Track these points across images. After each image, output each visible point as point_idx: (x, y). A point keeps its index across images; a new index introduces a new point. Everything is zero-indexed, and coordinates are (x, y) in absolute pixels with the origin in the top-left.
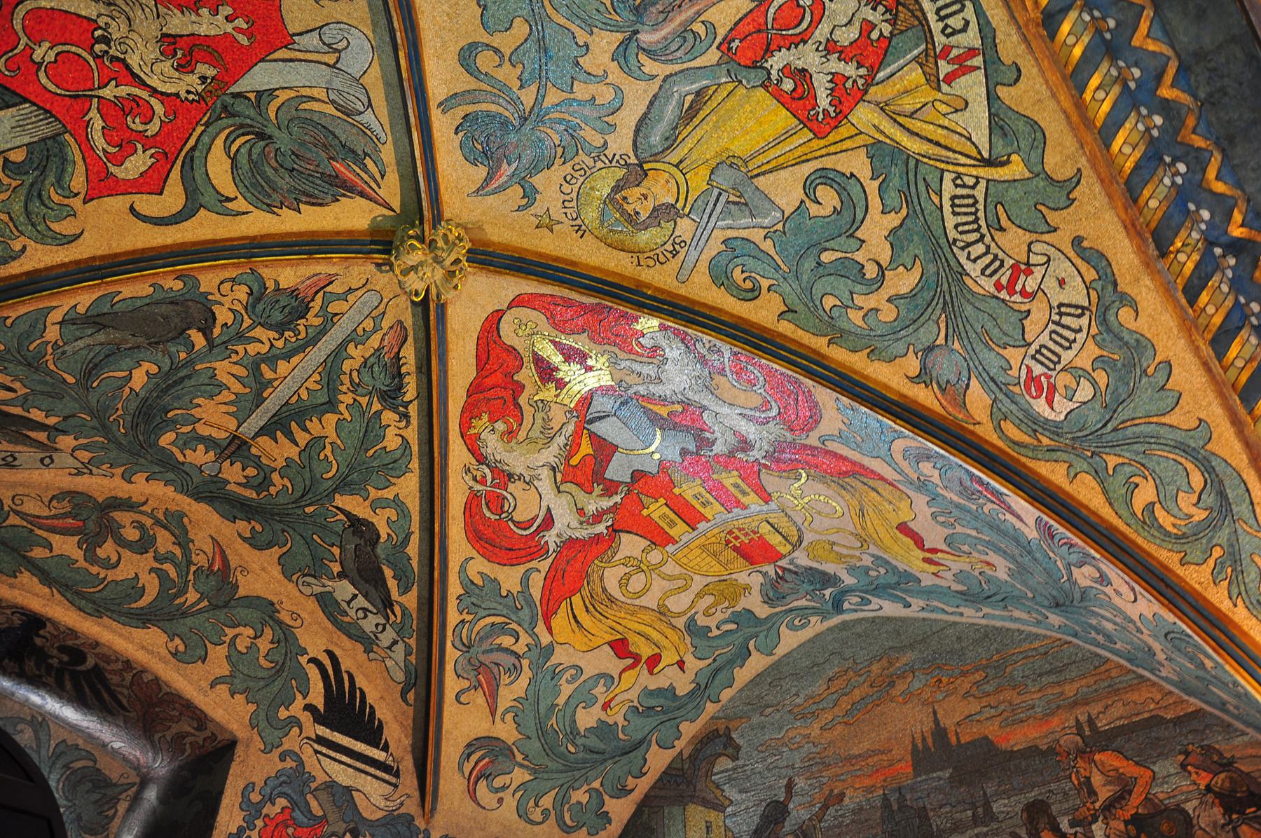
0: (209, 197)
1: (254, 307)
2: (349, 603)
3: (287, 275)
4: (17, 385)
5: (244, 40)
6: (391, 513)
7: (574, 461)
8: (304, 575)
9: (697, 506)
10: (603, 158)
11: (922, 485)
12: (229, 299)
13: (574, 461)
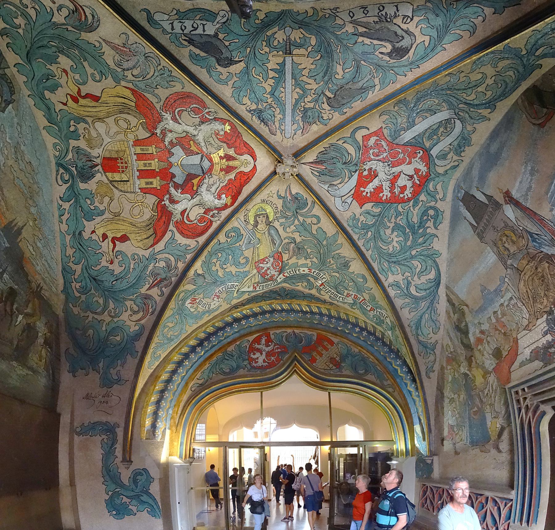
3: (316, 129)
5: (362, 189)
6: (223, 77)
7: (191, 142)
8: (228, 20)
9: (145, 162)
11: (153, 258)
13: (191, 142)
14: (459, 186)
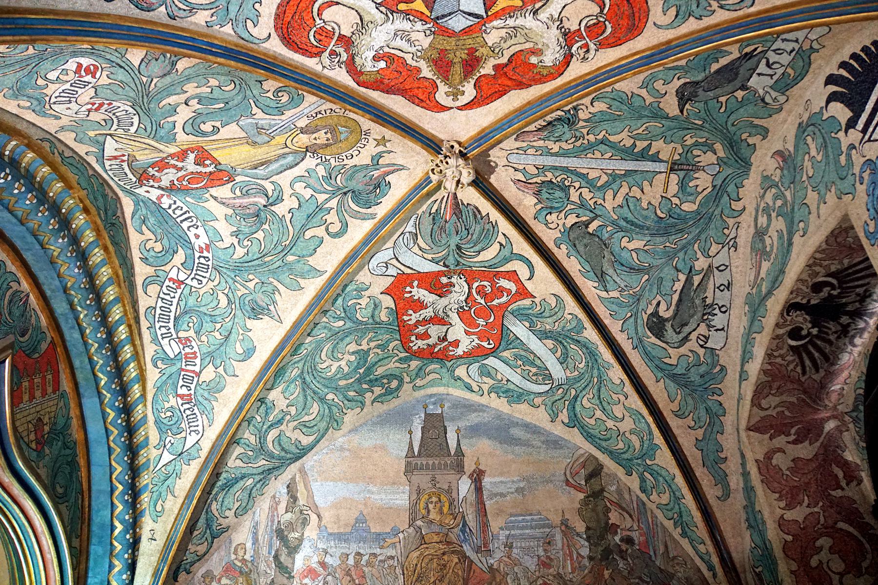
0: (506, 252)
1: (558, 208)
2: (771, 76)
4: (655, 302)
5: (416, 283)
10: (324, 159)
12: (559, 222)
14: (442, 400)
